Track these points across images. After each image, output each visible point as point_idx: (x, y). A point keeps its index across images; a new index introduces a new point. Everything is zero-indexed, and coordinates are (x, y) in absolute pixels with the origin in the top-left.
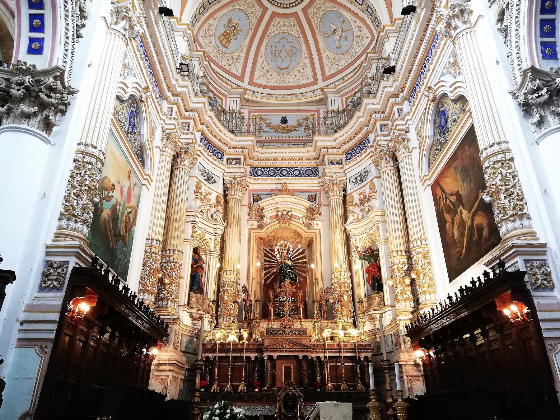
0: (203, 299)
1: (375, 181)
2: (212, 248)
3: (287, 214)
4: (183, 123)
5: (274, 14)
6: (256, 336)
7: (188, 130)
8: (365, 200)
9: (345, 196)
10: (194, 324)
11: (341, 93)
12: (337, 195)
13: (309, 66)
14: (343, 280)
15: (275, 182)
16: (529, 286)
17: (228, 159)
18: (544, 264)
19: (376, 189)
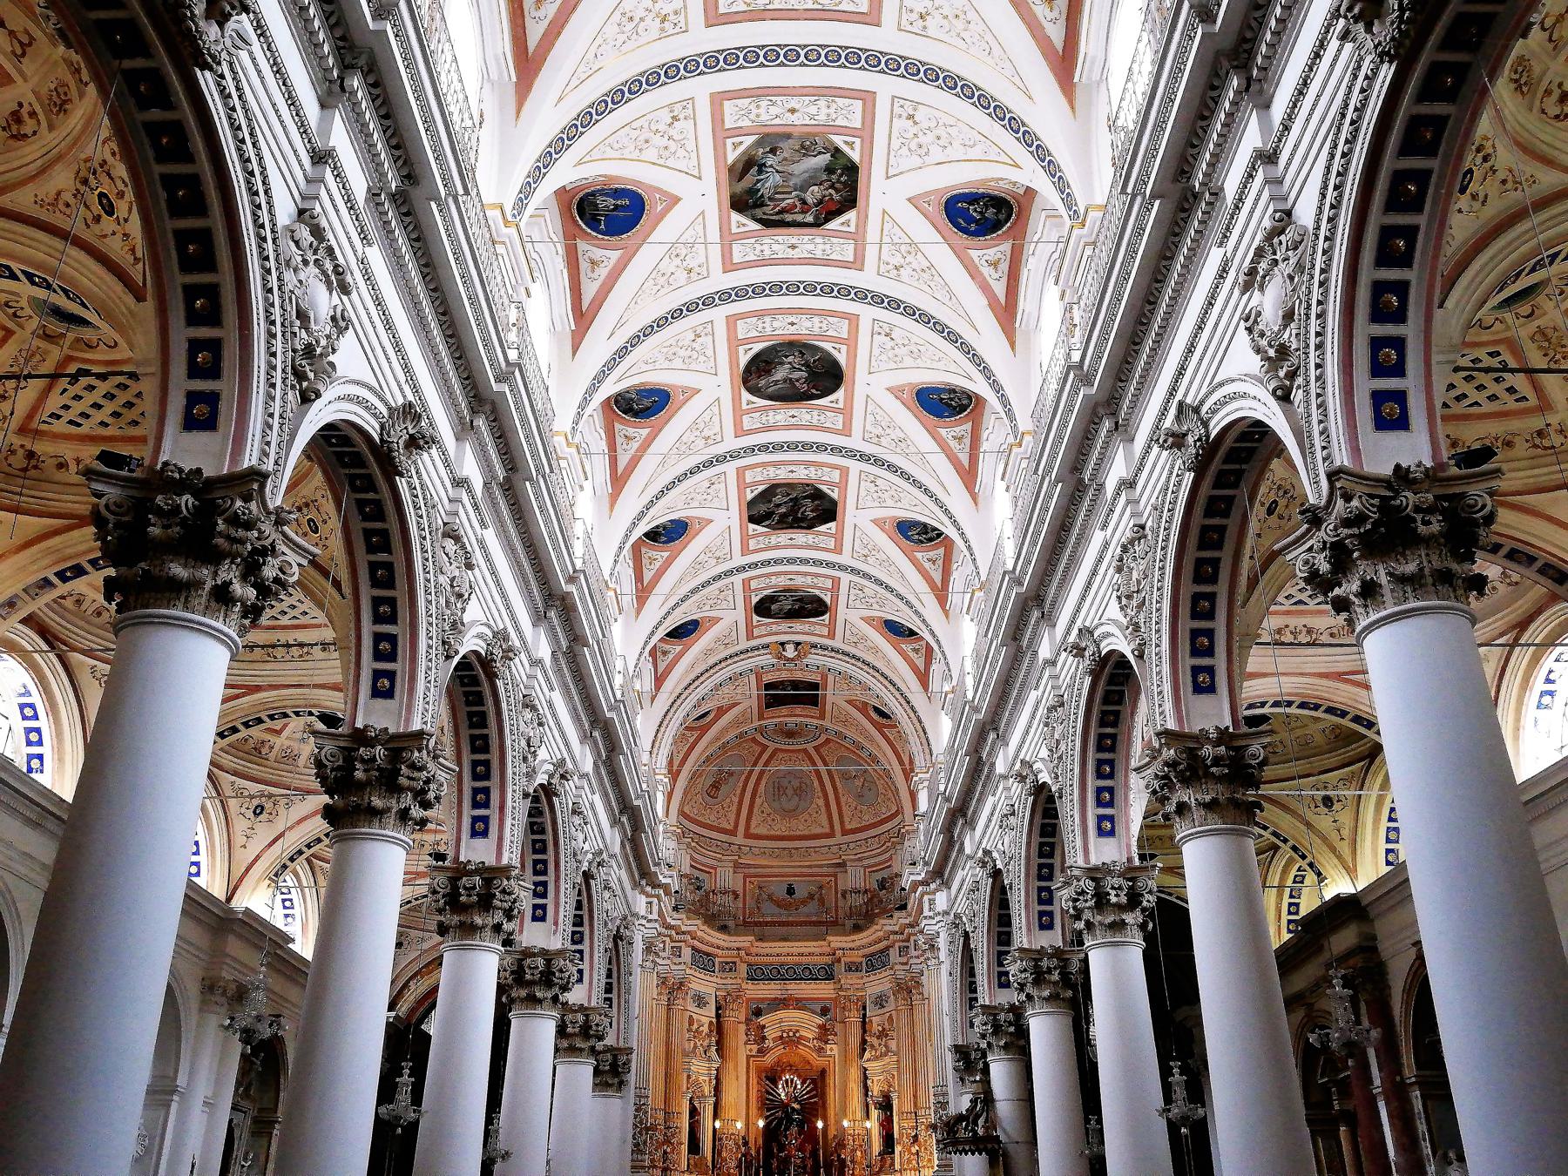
5: (776, 751)
9: (864, 1015)
11: (866, 862)
12: (854, 1018)
13: (823, 809)
17: (720, 963)
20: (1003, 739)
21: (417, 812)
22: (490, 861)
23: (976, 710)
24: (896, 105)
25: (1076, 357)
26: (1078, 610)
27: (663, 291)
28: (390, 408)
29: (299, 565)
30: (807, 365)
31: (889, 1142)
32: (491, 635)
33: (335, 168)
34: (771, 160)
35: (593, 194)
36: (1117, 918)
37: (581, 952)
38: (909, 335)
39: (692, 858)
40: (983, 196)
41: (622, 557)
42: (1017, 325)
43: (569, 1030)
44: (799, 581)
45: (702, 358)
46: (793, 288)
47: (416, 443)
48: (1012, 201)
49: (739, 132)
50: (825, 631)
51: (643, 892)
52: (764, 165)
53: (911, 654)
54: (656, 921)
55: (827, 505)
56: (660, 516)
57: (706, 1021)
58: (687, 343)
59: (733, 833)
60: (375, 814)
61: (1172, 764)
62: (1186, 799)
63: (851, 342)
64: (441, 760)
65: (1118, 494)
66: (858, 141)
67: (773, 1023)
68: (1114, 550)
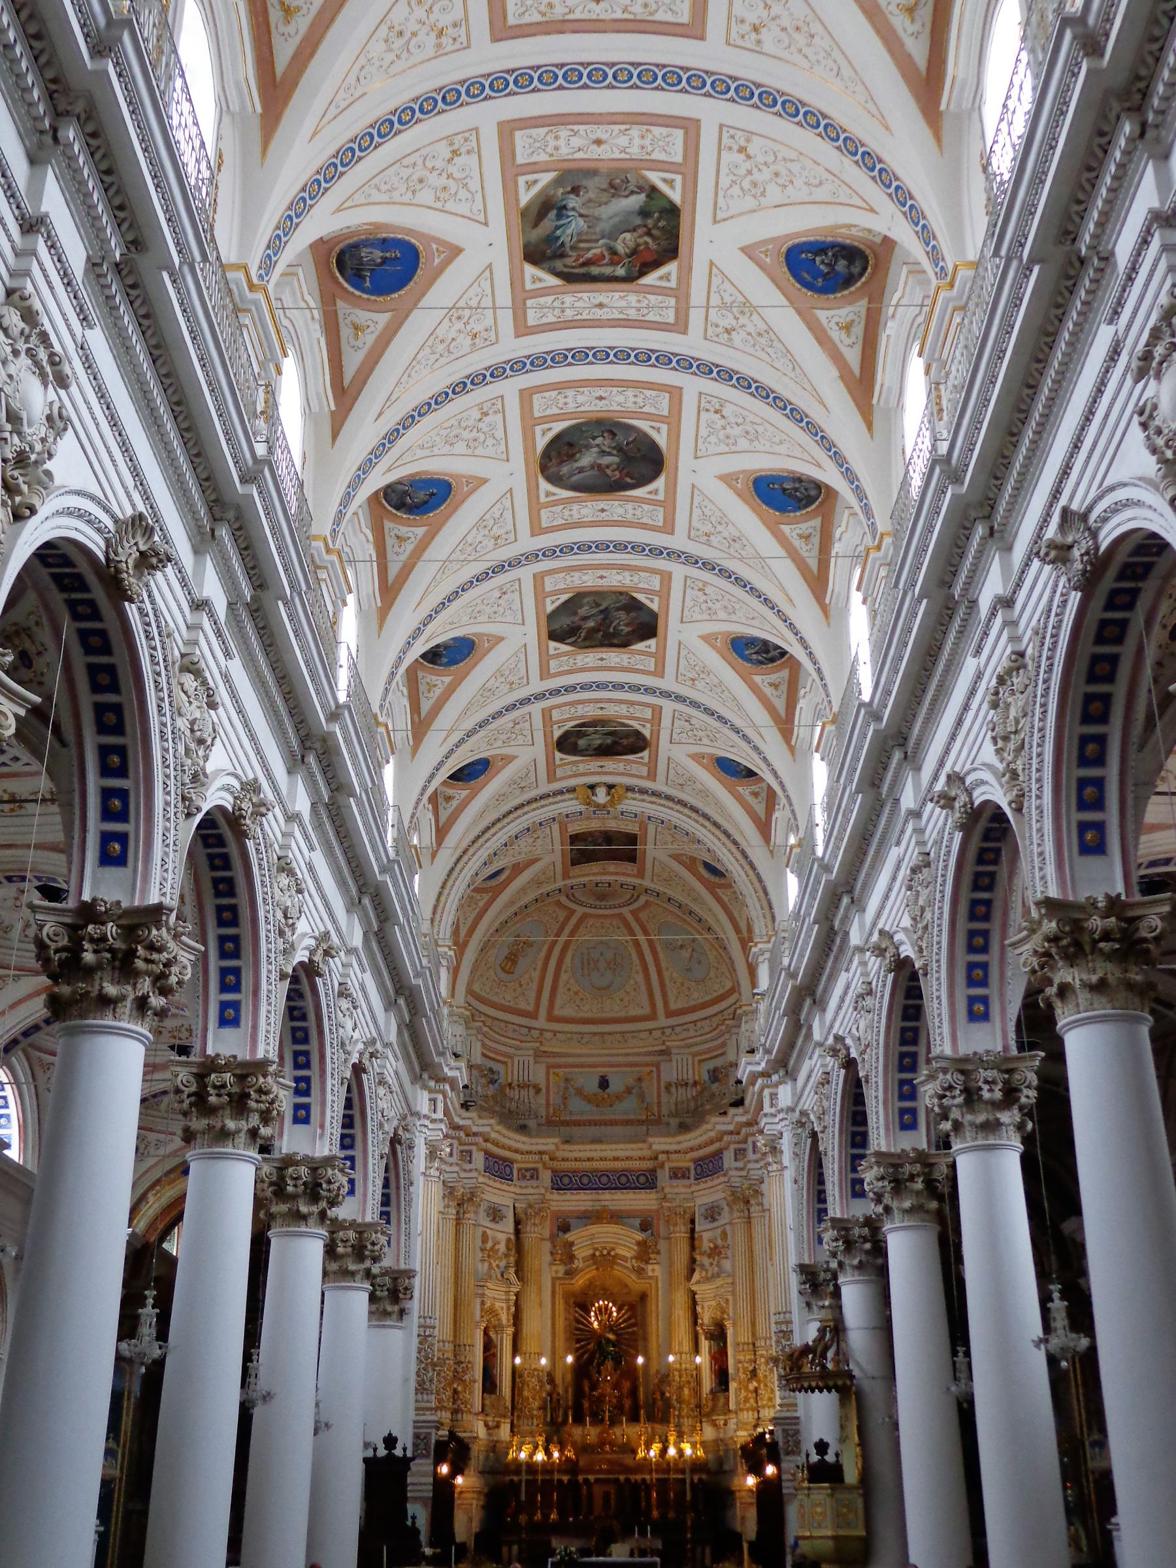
0: (499, 1400)
1: (728, 1228)
2: (504, 1321)
3: (609, 1253)
4: (462, 1152)
5: (584, 917)
6: (570, 1454)
7: (470, 1162)
8: (715, 1252)
9: (693, 1231)
10: (490, 1435)
12: (680, 1232)
13: (643, 988)
14: (683, 1366)
15: (590, 1197)
16: (782, 1452)
17: (519, 1170)
18: (797, 1432)
19: (729, 1241)
20: (858, 904)
21: (157, 1001)
22: (244, 1055)
23: (827, 869)
24: (725, 135)
25: (943, 448)
26: (947, 751)
27: (443, 361)
28: (116, 521)
29: (16, 716)
30: (620, 449)
31: (722, 1377)
32: (237, 785)
33: (49, 237)
34: (573, 202)
35: (356, 246)
36: (991, 1118)
37: (352, 1159)
38: (744, 413)
39: (484, 1045)
40: (833, 245)
41: (394, 683)
42: (875, 401)
43: (340, 1250)
44: (611, 711)
45: (490, 441)
46: (603, 355)
47: (150, 561)
48: (868, 252)
49: (534, 168)
50: (644, 771)
51: (425, 1087)
52: (564, 207)
53: (750, 799)
54: (441, 1121)
55: (644, 618)
56: (439, 633)
57: (502, 1238)
58: (471, 423)
59: (533, 1015)
60: (106, 1003)
61: (1054, 939)
62: (1070, 980)
63: (673, 420)
64: (184, 938)
65: (993, 614)
66: (678, 178)
67: (583, 1239)
68: (989, 682)
